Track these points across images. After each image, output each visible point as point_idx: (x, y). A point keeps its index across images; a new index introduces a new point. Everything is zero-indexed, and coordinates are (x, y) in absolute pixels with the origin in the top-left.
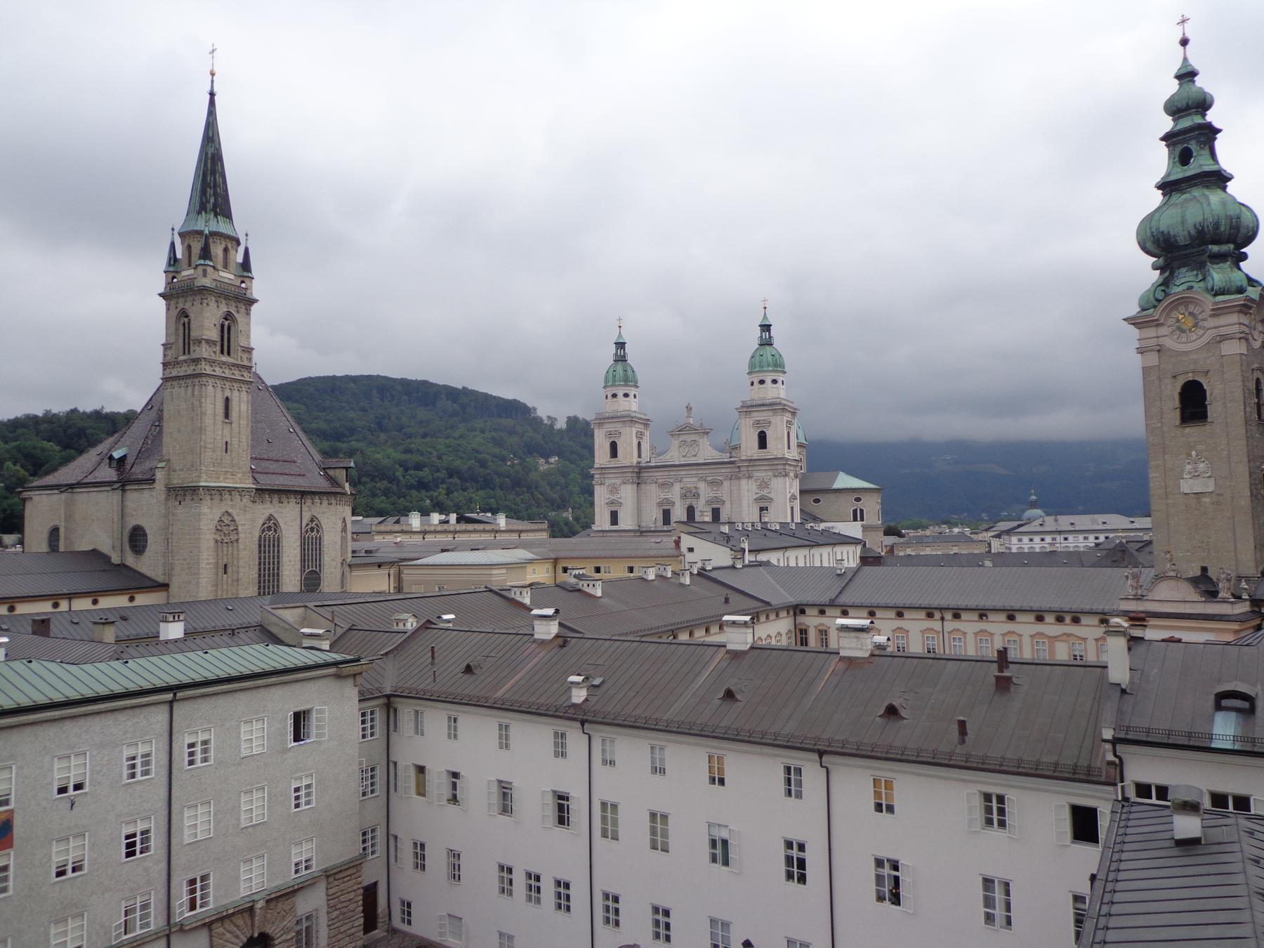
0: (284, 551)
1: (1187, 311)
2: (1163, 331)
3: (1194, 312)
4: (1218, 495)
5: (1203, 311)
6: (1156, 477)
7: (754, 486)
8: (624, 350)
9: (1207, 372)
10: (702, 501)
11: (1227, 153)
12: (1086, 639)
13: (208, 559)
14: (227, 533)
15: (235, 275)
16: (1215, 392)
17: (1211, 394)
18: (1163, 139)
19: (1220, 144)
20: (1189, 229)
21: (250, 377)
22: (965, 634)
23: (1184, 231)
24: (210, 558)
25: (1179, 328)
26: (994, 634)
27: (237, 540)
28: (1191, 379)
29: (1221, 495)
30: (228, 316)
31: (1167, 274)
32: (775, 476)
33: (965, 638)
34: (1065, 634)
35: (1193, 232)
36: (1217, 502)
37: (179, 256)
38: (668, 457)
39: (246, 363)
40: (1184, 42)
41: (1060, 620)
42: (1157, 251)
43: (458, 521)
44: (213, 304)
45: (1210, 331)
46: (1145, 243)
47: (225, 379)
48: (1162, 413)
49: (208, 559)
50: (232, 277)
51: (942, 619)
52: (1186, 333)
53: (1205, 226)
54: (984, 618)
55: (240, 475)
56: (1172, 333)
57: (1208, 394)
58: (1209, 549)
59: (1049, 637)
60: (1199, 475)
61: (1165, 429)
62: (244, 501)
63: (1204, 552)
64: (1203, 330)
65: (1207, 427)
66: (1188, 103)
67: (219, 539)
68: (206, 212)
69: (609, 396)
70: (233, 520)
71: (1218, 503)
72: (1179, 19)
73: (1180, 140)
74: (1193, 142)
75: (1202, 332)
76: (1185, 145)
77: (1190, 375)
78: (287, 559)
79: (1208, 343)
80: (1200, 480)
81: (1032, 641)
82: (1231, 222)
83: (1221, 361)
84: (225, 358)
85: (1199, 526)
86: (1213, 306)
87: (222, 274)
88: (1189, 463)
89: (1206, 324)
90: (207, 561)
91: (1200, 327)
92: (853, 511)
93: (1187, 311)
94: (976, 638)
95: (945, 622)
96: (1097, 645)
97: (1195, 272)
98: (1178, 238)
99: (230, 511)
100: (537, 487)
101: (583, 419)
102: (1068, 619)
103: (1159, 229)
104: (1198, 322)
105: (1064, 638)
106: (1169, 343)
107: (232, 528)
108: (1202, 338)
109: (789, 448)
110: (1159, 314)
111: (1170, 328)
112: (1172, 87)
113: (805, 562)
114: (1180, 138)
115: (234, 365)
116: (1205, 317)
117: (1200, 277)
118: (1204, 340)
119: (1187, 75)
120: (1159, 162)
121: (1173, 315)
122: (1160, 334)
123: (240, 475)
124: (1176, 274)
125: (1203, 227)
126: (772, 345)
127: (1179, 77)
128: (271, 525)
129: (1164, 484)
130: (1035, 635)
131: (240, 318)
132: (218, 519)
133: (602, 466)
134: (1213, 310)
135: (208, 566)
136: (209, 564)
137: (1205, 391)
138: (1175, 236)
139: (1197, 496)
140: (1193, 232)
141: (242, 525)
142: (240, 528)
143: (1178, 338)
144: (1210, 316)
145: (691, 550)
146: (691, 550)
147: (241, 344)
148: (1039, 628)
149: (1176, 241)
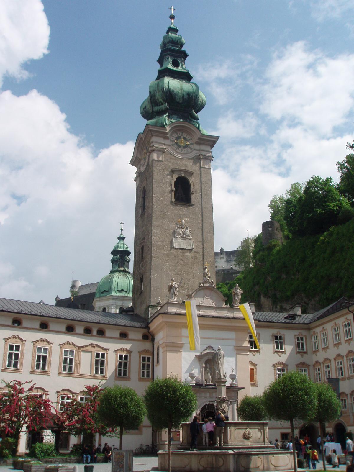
1: (182, 135)
2: (168, 142)
3: (187, 138)
4: (195, 252)
5: (191, 139)
6: (156, 233)
9: (192, 174)
12: (109, 349)
20: (184, 94)
23: (181, 94)
25: (177, 143)
26: (25, 341)
28: (183, 175)
29: (197, 252)
34: (91, 344)
35: (186, 97)
41: (88, 331)
45: (194, 151)
46: (155, 92)
52: (181, 148)
54: (16, 325)
56: (172, 145)
57: (192, 187)
60: (185, 237)
63: (184, 291)
65: (191, 208)
66: (178, 40)
73: (173, 54)
74: (179, 59)
75: (190, 151)
76: (176, 58)
77: (183, 173)
80: (184, 241)
82: (202, 102)
86: (200, 136)
89: (192, 147)
91: (189, 147)
93: (182, 135)
98: (177, 97)
102: (95, 332)
108: (191, 154)
111: (172, 142)
114: (173, 53)
116: (192, 143)
122: (166, 143)
125: (192, 96)
134: (199, 139)
137: (190, 185)
138: (175, 94)
139: (182, 251)
140: (186, 97)
143: (176, 149)
144: (195, 143)
149: (175, 98)
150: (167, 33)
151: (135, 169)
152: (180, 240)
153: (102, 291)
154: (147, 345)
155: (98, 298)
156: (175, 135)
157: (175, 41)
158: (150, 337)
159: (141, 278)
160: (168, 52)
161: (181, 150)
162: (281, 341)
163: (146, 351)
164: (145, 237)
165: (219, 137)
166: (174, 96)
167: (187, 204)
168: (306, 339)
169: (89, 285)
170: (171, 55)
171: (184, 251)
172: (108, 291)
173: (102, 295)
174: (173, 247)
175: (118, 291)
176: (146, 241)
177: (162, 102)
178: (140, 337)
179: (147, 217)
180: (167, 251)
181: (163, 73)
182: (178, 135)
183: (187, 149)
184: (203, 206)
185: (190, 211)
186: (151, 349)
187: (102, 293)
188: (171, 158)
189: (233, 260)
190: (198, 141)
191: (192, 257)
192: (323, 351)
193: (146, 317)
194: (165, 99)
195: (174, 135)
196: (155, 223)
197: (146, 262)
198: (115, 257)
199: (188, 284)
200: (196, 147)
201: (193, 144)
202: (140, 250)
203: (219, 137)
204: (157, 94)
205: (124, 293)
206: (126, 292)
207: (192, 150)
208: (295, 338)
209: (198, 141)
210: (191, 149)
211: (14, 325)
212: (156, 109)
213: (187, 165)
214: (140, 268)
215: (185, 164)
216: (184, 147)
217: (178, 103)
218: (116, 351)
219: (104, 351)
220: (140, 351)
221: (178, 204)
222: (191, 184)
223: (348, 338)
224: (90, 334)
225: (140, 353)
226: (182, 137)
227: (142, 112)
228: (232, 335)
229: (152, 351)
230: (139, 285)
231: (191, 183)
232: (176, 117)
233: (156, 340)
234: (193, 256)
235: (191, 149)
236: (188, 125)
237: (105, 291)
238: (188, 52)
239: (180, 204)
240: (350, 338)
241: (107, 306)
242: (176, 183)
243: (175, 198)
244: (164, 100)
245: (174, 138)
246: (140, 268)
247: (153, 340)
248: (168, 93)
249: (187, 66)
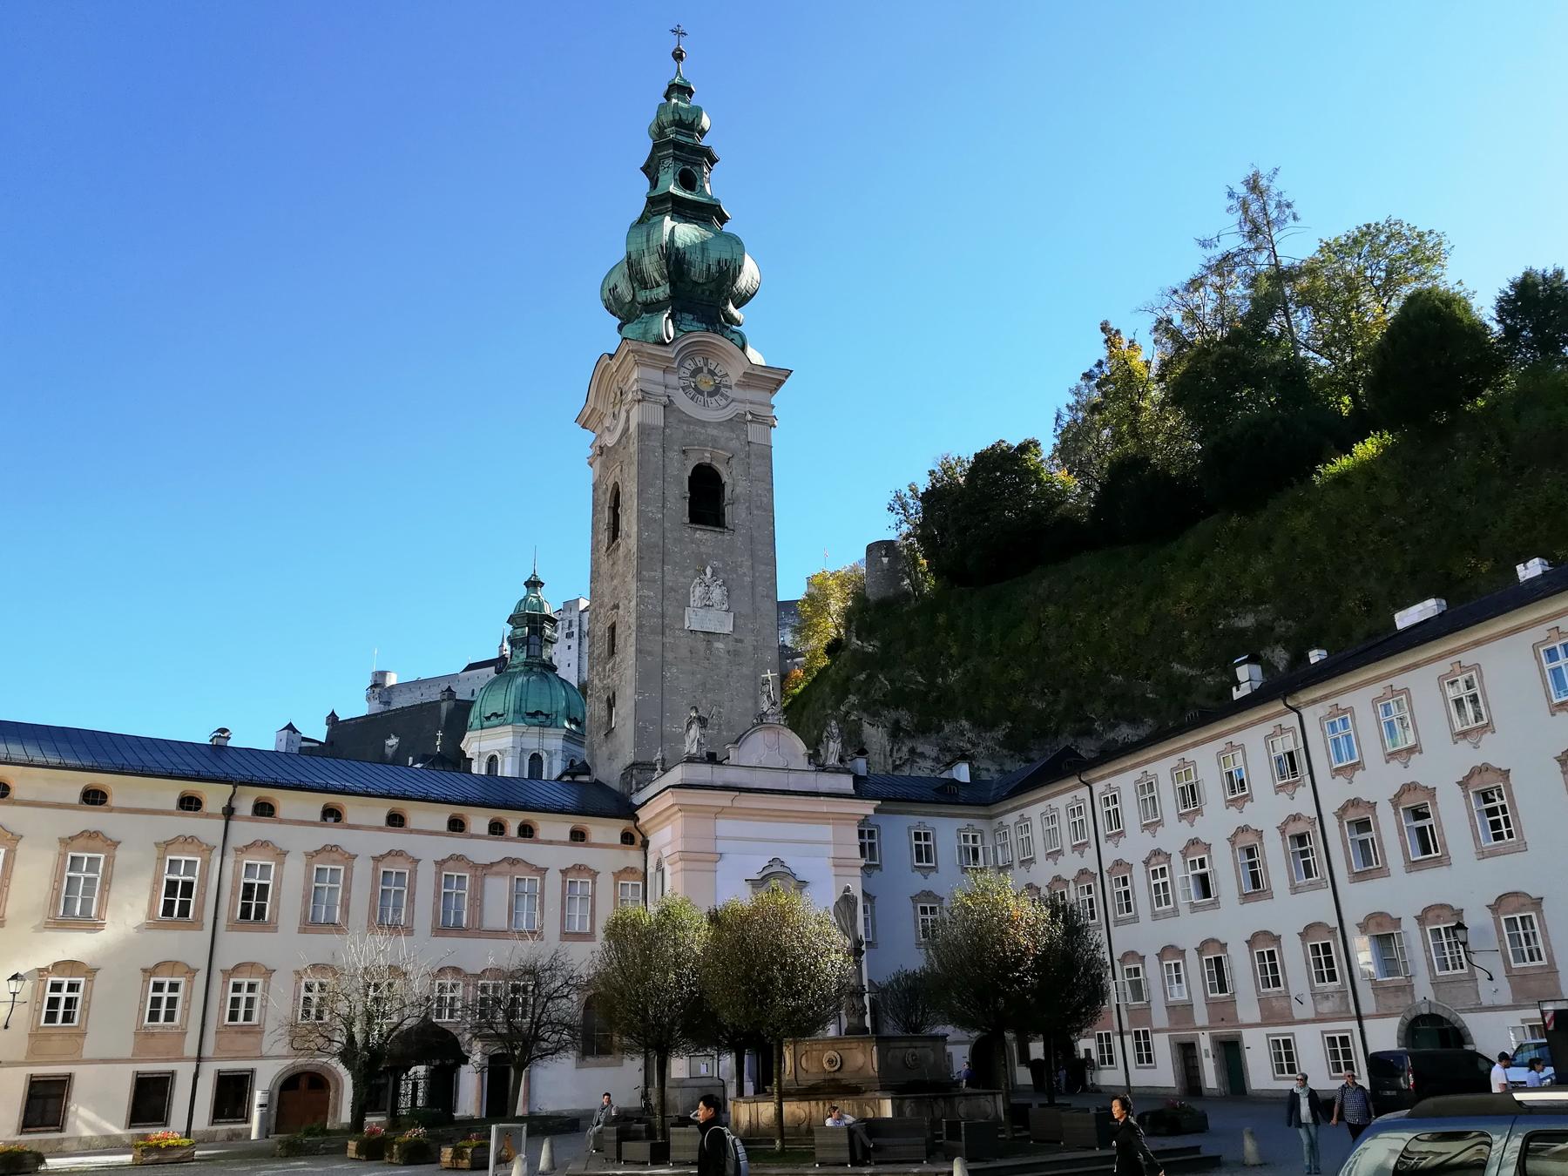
2: (673, 379)
4: (737, 641)
16: (738, 490)
22: (281, 855)
28: (708, 461)
29: (741, 641)
33: (281, 864)
35: (714, 268)
36: (735, 651)
45: (733, 404)
48: (664, 499)
51: (229, 812)
53: (731, 268)
54: (331, 820)
57: (728, 490)
58: (720, 725)
59: (475, 866)
60: (713, 606)
61: (667, 525)
71: (736, 653)
72: (674, 27)
75: (723, 403)
79: (731, 419)
80: (712, 614)
81: (438, 874)
83: (747, 449)
85: (708, 686)
89: (729, 392)
91: (722, 395)
93: (705, 365)
94: (309, 866)
95: (232, 823)
96: (564, 882)
98: (693, 269)
105: (506, 866)
106: (683, 401)
110: (676, 351)
116: (728, 383)
118: (728, 413)
121: (686, 365)
129: (660, 610)
130: (444, 861)
138: (690, 263)
139: (707, 637)
148: (456, 845)
150: (668, 96)
151: (589, 436)
152: (702, 612)
153: (488, 715)
154: (633, 857)
155: (477, 730)
156: (690, 365)
157: (687, 122)
158: (638, 839)
159: (608, 697)
160: (671, 151)
161: (702, 400)
162: (927, 843)
163: (629, 871)
164: (618, 604)
165: (791, 371)
166: (686, 266)
167: (717, 529)
168: (982, 838)
169: (419, 683)
170: (676, 158)
171: (710, 637)
172: (502, 715)
173: (486, 724)
174: (686, 628)
175: (528, 714)
176: (621, 612)
177: (658, 279)
178: (618, 840)
179: (625, 557)
180: (674, 637)
181: (658, 205)
183: (716, 398)
184: (755, 534)
185: (725, 546)
186: (640, 867)
187: (488, 718)
188: (679, 421)
189: (786, 624)
190: (743, 379)
191: (729, 652)
192: (1023, 867)
193: (626, 790)
194: (666, 272)
195: (686, 365)
196: (645, 573)
197: (622, 661)
198: (519, 631)
199: (719, 712)
200: (736, 393)
201: (730, 388)
202: (604, 631)
203: (791, 371)
204: (646, 260)
205: (542, 718)
206: (547, 716)
207: (729, 400)
208: (959, 837)
209: (743, 379)
211: (326, 820)
212: (643, 296)
213: (717, 436)
214: (607, 674)
215: (712, 436)
216: (711, 394)
217: (696, 283)
218: (564, 872)
219: (534, 873)
220: (616, 871)
221: (697, 529)
223: (1078, 842)
224: (503, 836)
225: (618, 875)
226: (705, 370)
227: (605, 297)
228: (826, 831)
229: (643, 870)
230: (604, 713)
231: (725, 478)
232: (691, 317)
233: (651, 847)
234: (731, 649)
235: (727, 398)
236: (718, 340)
237: (495, 714)
238: (717, 152)
239: (701, 529)
240: (1083, 840)
241: (500, 752)
242: (690, 479)
243: (690, 516)
244: (663, 277)
245: (688, 372)
246: (607, 674)
247: (645, 845)
248: (673, 258)
249: (714, 185)
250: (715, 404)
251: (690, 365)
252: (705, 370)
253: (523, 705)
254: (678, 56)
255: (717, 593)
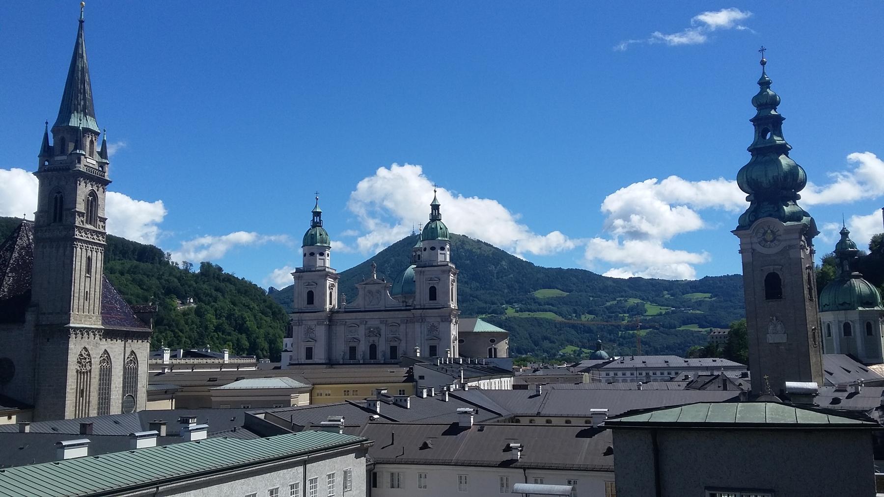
0: (112, 379)
7: (426, 329)
8: (320, 218)
10: (383, 339)
11: (789, 134)
13: (71, 385)
14: (84, 364)
15: (97, 162)
17: (784, 281)
18: (751, 121)
19: (784, 127)
21: (104, 241)
24: (73, 384)
27: (90, 371)
28: (772, 271)
30: (93, 194)
31: (755, 205)
32: (442, 321)
35: (772, 181)
37: (51, 143)
38: (355, 305)
39: (101, 230)
40: (763, 63)
42: (750, 190)
43: (185, 356)
44: (83, 184)
47: (95, 244)
49: (71, 385)
50: (94, 162)
55: (94, 318)
62: (96, 338)
64: (779, 241)
67: (79, 369)
68: (77, 112)
69: (308, 254)
70: (89, 355)
78: (114, 386)
84: (89, 226)
87: (88, 160)
88: (772, 325)
90: (70, 387)
92: (489, 349)
97: (773, 206)
99: (87, 347)
100: (177, 325)
101: (216, 265)
103: (751, 177)
104: (776, 237)
106: (759, 248)
107: (87, 360)
109: (452, 301)
110: (752, 230)
112: (757, 89)
113: (501, 386)
115: (94, 231)
117: (776, 209)
119: (764, 84)
120: (749, 135)
123: (94, 318)
124: (761, 205)
125: (778, 178)
126: (440, 220)
127: (759, 83)
128: (106, 358)
131: (99, 194)
132: (79, 353)
133: (300, 311)
135: (71, 391)
136: (72, 389)
137: (780, 280)
141: (94, 358)
142: (92, 360)
145: (422, 377)
146: (422, 377)
147: (99, 215)
175: (840, 304)
182: (765, 230)
183: (775, 242)
201: (780, 236)
206: (849, 304)
210: (779, 240)
216: (771, 241)
222: (781, 279)
226: (769, 231)
232: (767, 203)
235: (779, 240)
250: (774, 245)
251: (762, 231)
252: (769, 231)
253: (836, 300)
254: (763, 63)
255: (779, 327)
